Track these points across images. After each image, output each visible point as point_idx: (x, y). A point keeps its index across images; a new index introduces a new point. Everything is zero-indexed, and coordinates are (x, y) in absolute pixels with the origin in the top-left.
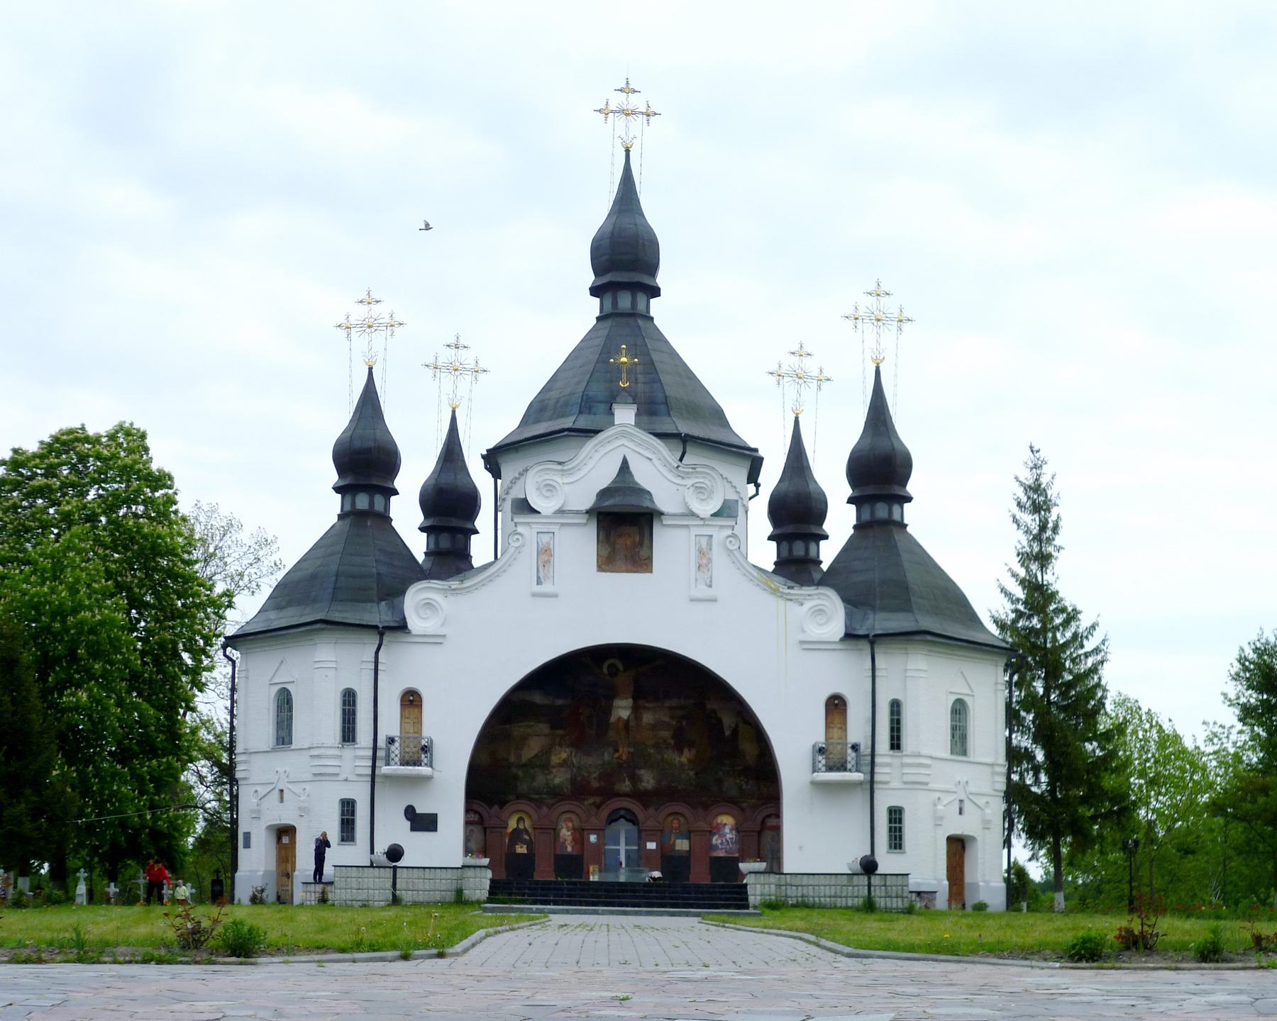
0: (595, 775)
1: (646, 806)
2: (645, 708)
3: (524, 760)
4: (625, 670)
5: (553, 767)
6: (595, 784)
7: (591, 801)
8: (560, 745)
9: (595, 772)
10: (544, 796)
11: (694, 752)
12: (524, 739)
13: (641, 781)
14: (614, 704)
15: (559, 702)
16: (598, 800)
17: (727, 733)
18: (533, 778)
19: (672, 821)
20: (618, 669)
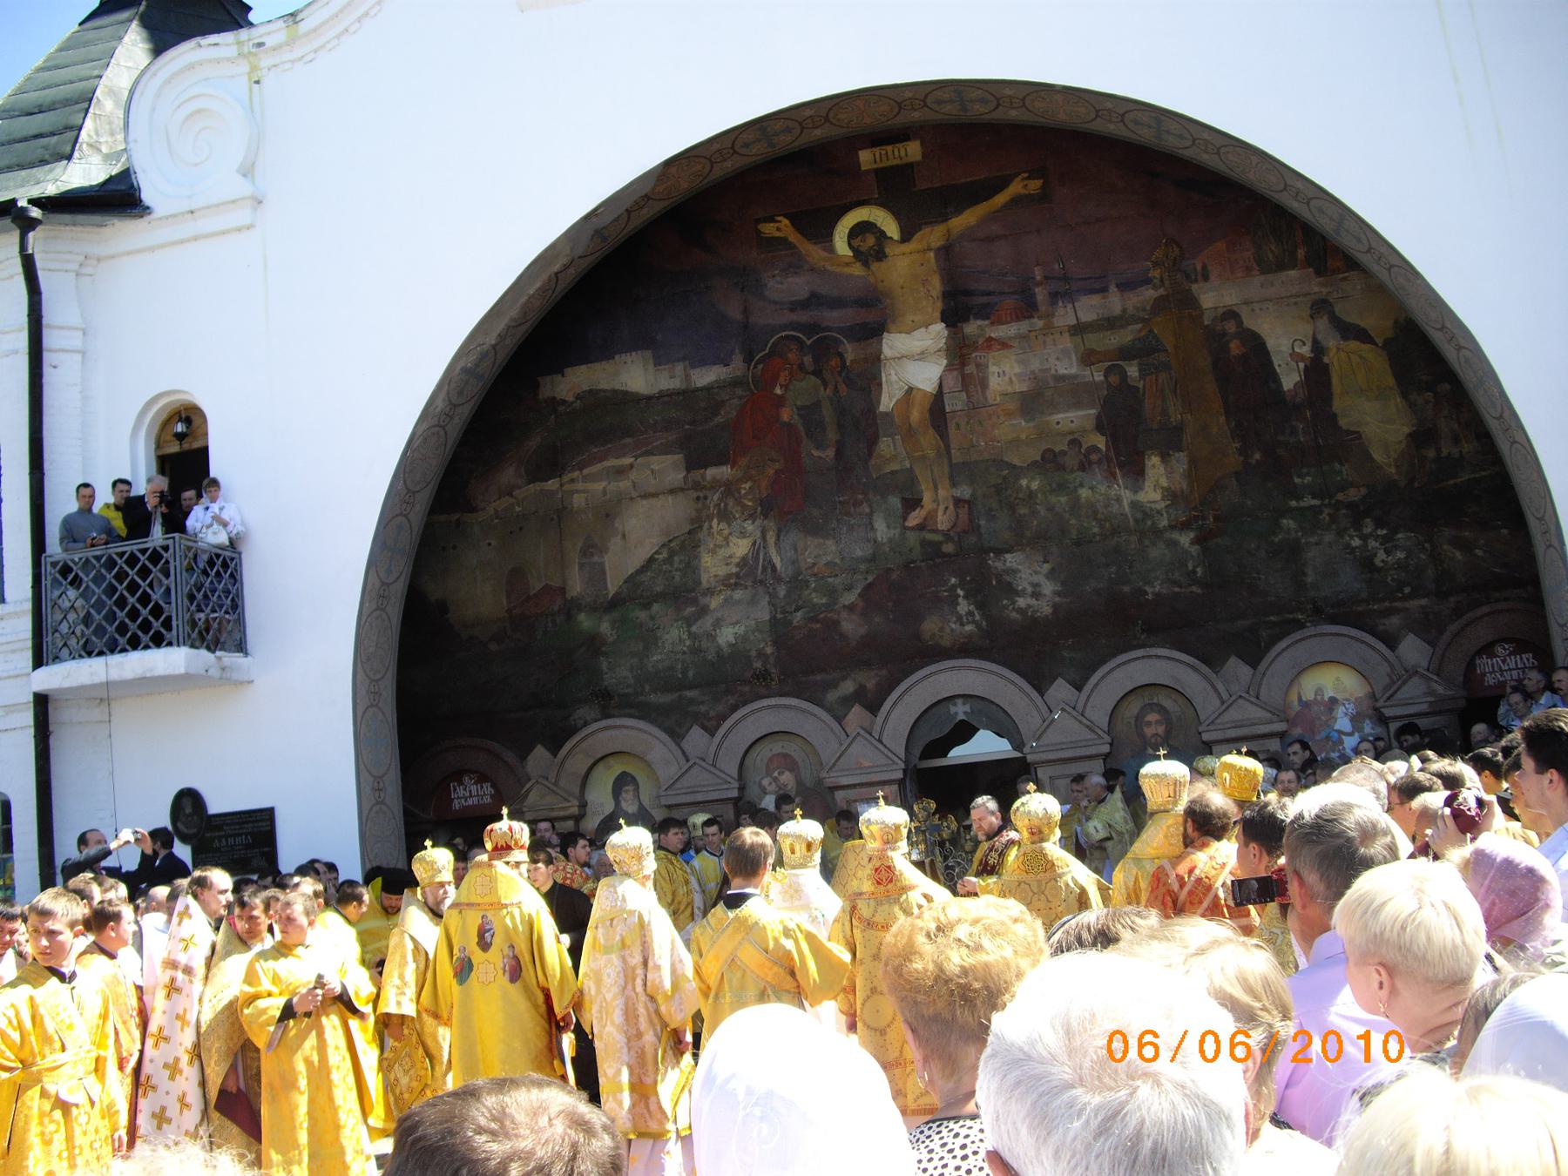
0: (850, 598)
1: (1040, 683)
2: (990, 343)
3: (612, 586)
4: (906, 237)
5: (710, 592)
6: (851, 626)
7: (848, 687)
8: (725, 516)
9: (849, 588)
10: (690, 694)
11: (1180, 461)
12: (608, 513)
13: (1011, 591)
14: (887, 351)
15: (705, 377)
16: (870, 679)
17: (1290, 380)
18: (650, 638)
19: (1139, 718)
20: (883, 233)
